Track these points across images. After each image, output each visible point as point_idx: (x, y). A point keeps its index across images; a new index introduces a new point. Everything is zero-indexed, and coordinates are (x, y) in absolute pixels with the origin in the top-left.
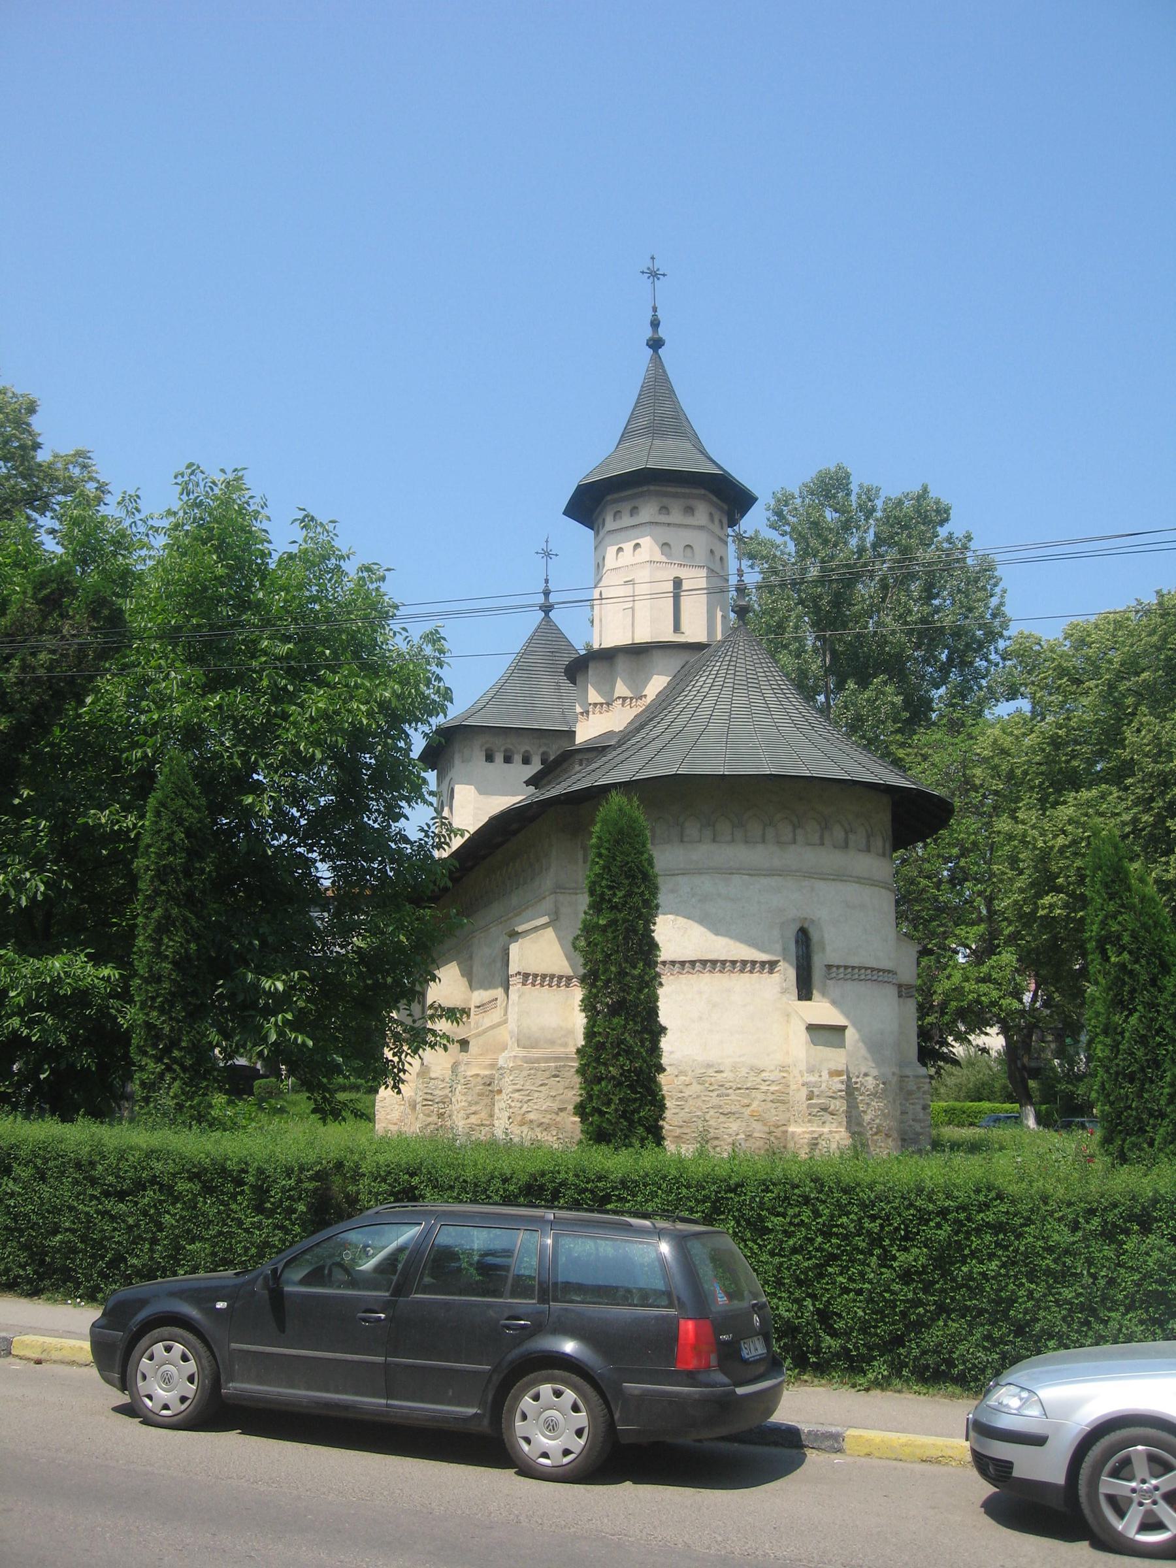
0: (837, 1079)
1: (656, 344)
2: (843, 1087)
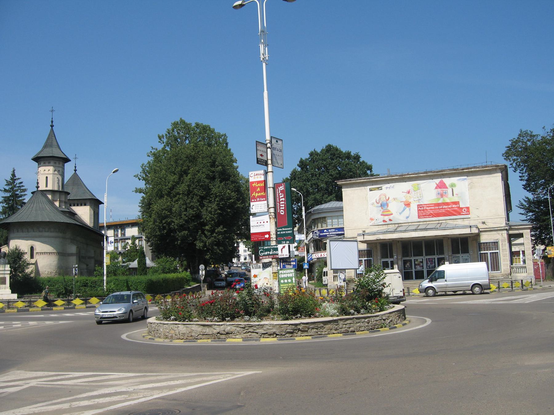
1: (52, 126)
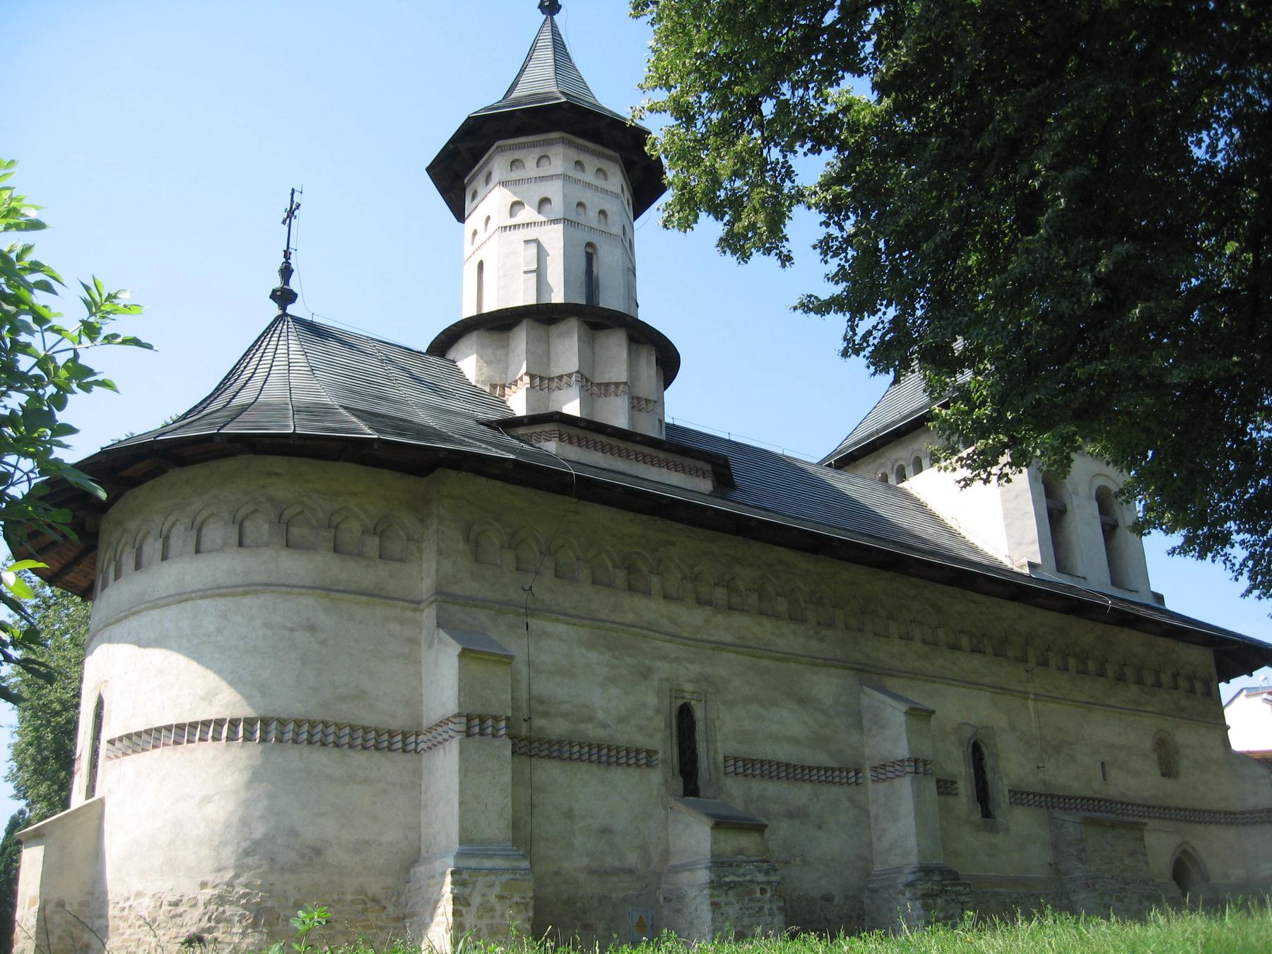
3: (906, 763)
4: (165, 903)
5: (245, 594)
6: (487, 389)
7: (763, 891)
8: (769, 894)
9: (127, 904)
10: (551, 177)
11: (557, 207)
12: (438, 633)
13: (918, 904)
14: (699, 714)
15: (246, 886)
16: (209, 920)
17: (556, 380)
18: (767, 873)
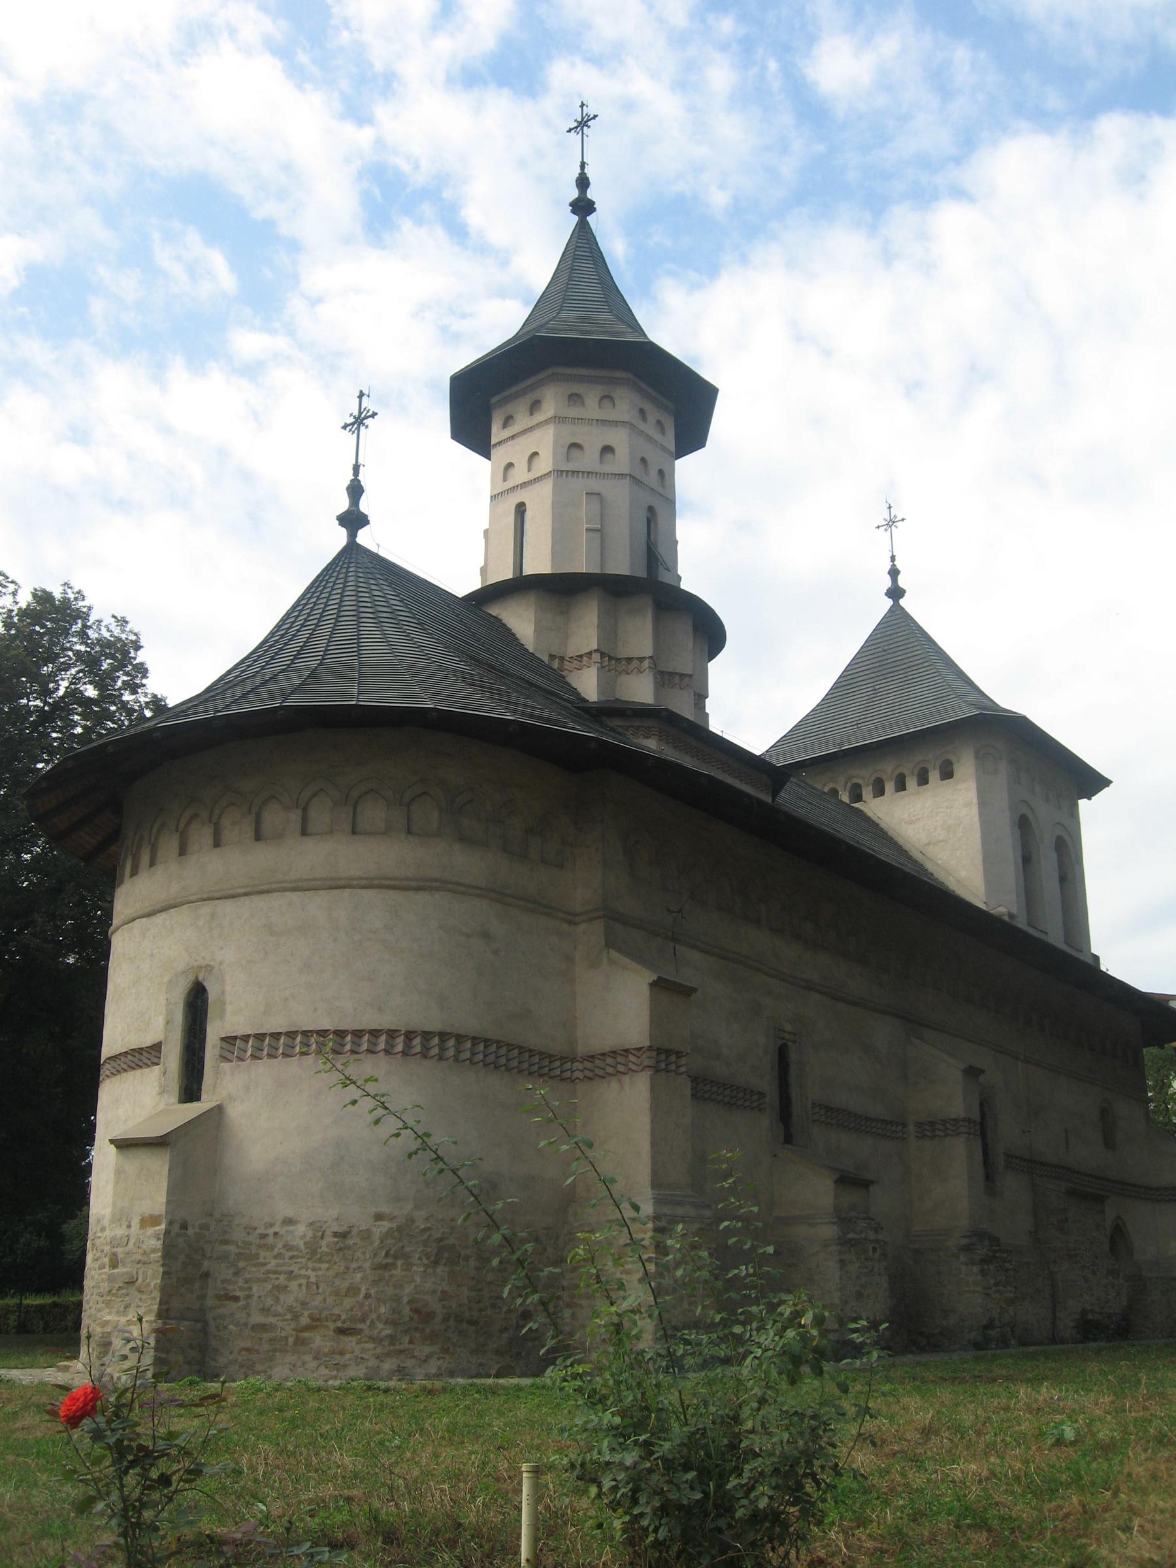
0: (151, 1231)
2: (158, 1244)
3: (961, 1123)
4: (328, 1232)
5: (418, 889)
6: (546, 659)
7: (874, 1249)
8: (878, 1252)
9: (271, 1231)
10: (615, 423)
11: (622, 462)
12: (608, 953)
13: (975, 1269)
14: (793, 1056)
15: (427, 1219)
16: (387, 1255)
17: (624, 662)
18: (876, 1232)
